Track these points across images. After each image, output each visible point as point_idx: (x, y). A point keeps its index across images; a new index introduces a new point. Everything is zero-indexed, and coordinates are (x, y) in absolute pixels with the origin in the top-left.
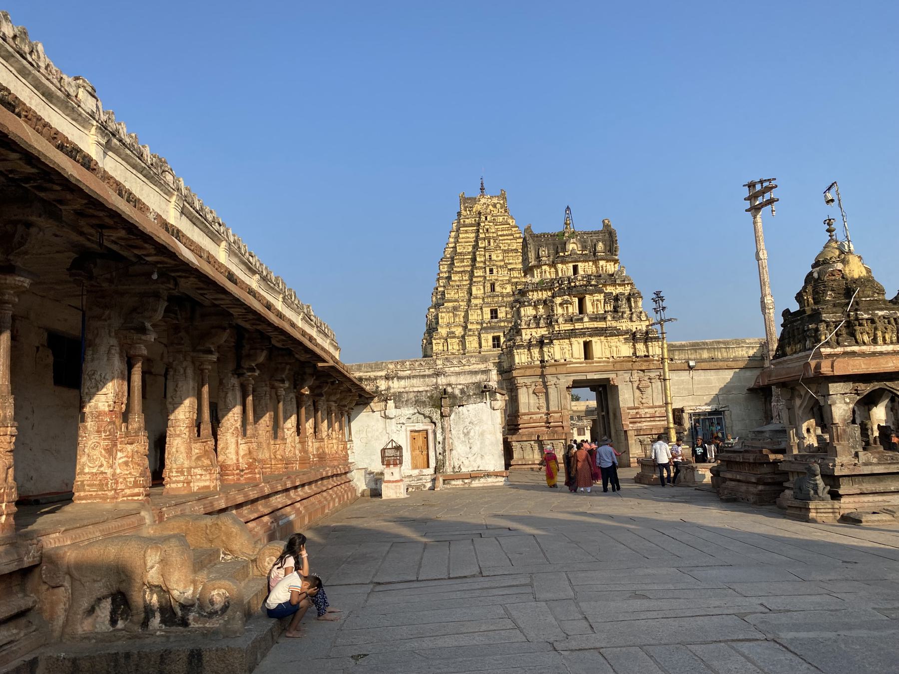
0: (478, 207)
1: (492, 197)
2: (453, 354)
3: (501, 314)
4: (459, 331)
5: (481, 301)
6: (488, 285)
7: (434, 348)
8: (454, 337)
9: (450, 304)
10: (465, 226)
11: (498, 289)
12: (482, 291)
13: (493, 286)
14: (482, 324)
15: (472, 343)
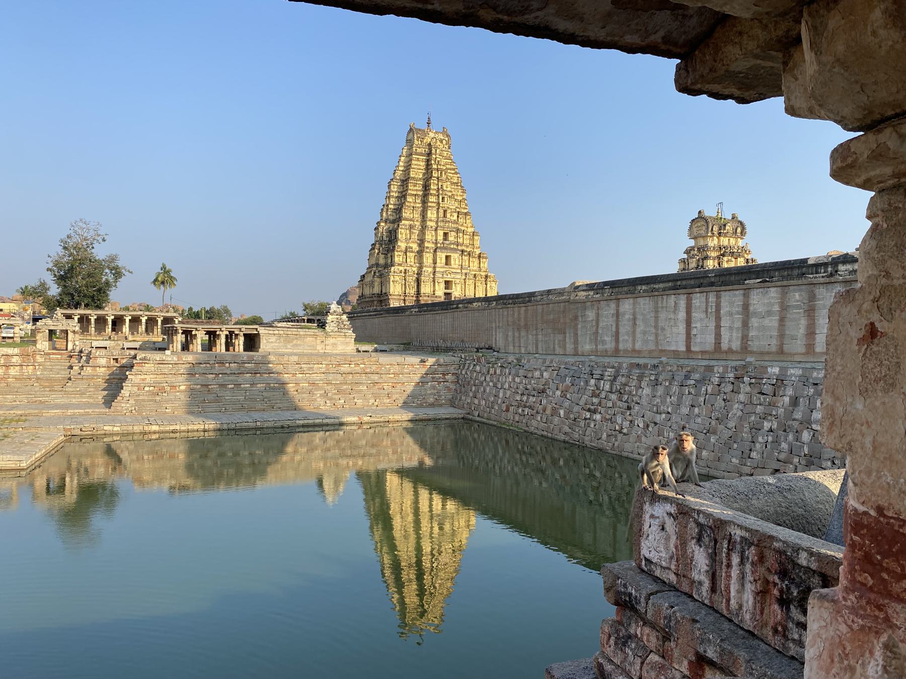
0: (427, 140)
1: (436, 133)
2: (411, 266)
3: (452, 237)
4: (415, 247)
5: (433, 224)
6: (441, 211)
7: (396, 259)
8: (412, 252)
9: (407, 223)
10: (417, 154)
11: (448, 215)
12: (435, 215)
13: (445, 212)
14: (436, 243)
15: (428, 258)
